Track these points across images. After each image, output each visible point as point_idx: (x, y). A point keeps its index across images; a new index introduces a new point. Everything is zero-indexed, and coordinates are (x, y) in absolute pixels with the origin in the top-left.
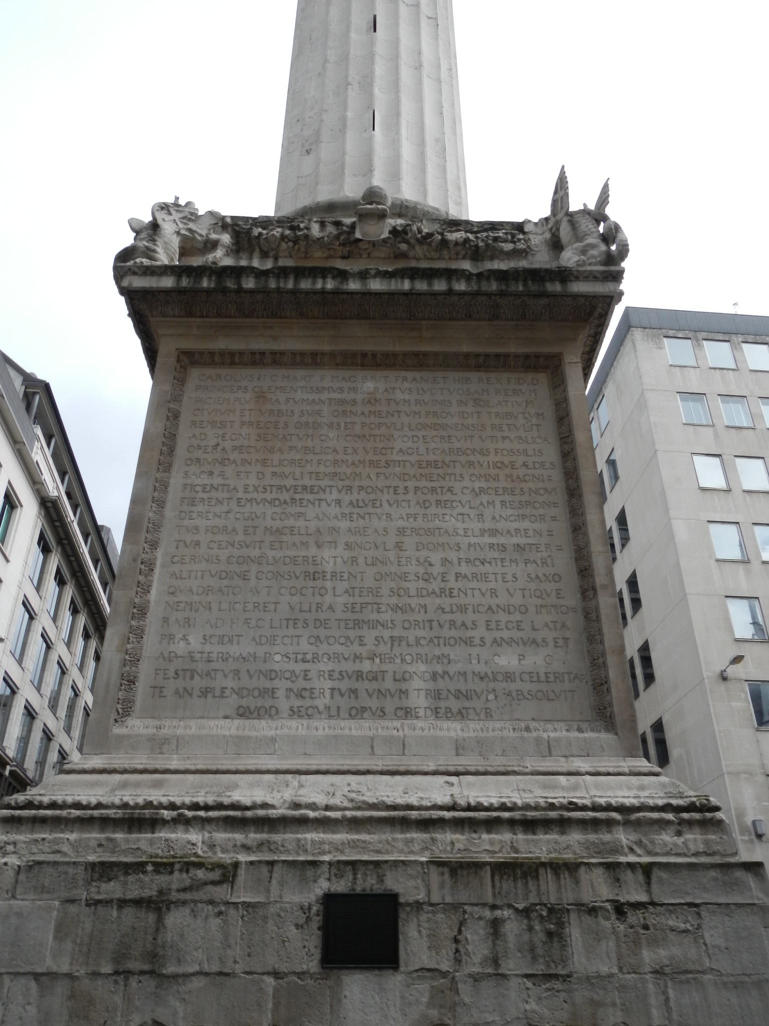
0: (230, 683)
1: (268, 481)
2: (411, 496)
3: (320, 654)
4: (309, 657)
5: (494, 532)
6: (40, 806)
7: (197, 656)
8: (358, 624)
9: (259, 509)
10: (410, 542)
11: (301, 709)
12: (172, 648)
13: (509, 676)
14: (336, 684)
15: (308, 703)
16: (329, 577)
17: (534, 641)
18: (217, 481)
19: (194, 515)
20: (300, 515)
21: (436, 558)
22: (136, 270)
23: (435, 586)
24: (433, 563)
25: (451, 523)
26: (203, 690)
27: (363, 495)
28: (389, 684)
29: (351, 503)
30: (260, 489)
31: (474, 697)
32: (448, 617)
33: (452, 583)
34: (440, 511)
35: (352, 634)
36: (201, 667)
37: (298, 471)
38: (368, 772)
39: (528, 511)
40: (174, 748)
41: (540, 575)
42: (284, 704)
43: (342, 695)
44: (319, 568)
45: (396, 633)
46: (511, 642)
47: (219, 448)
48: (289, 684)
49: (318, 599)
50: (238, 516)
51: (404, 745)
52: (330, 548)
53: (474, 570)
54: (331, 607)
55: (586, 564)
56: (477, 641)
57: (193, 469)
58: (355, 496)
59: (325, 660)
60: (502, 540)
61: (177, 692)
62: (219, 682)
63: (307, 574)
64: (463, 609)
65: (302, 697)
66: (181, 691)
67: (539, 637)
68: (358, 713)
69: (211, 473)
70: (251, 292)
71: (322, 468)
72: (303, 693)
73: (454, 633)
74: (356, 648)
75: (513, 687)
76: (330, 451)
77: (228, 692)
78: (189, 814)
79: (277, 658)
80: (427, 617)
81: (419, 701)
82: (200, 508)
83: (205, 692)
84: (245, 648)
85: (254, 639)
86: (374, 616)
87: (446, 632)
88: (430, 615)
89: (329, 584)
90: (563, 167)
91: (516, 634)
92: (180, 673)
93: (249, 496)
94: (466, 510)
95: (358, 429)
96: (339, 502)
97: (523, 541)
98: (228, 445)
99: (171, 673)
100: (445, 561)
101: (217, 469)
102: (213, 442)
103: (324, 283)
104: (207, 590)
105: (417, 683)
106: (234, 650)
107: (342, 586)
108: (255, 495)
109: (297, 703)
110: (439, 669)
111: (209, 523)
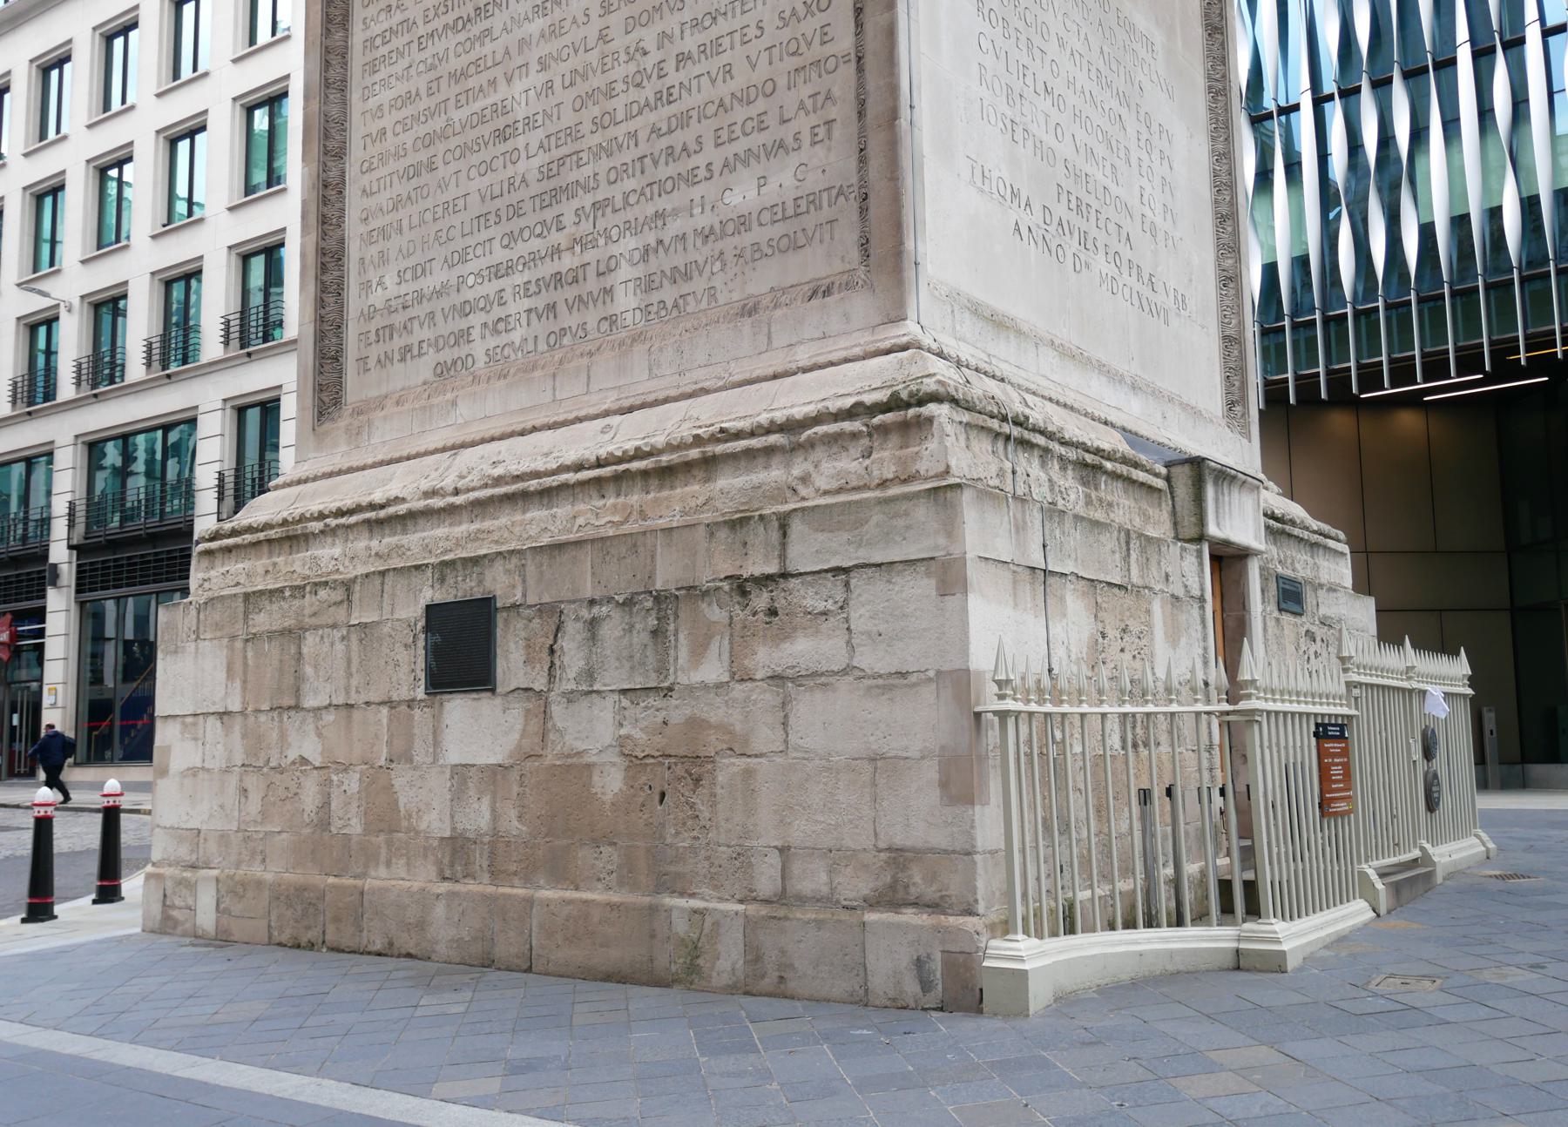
0: (427, 333)
13: (743, 223)
32: (664, 142)
33: (673, 78)
46: (746, 158)
56: (702, 173)
67: (787, 133)
74: (556, 238)
75: (747, 239)
78: (333, 522)
80: (639, 153)
87: (663, 172)
91: (756, 140)
99: (373, 337)
105: (625, 272)
106: (428, 283)
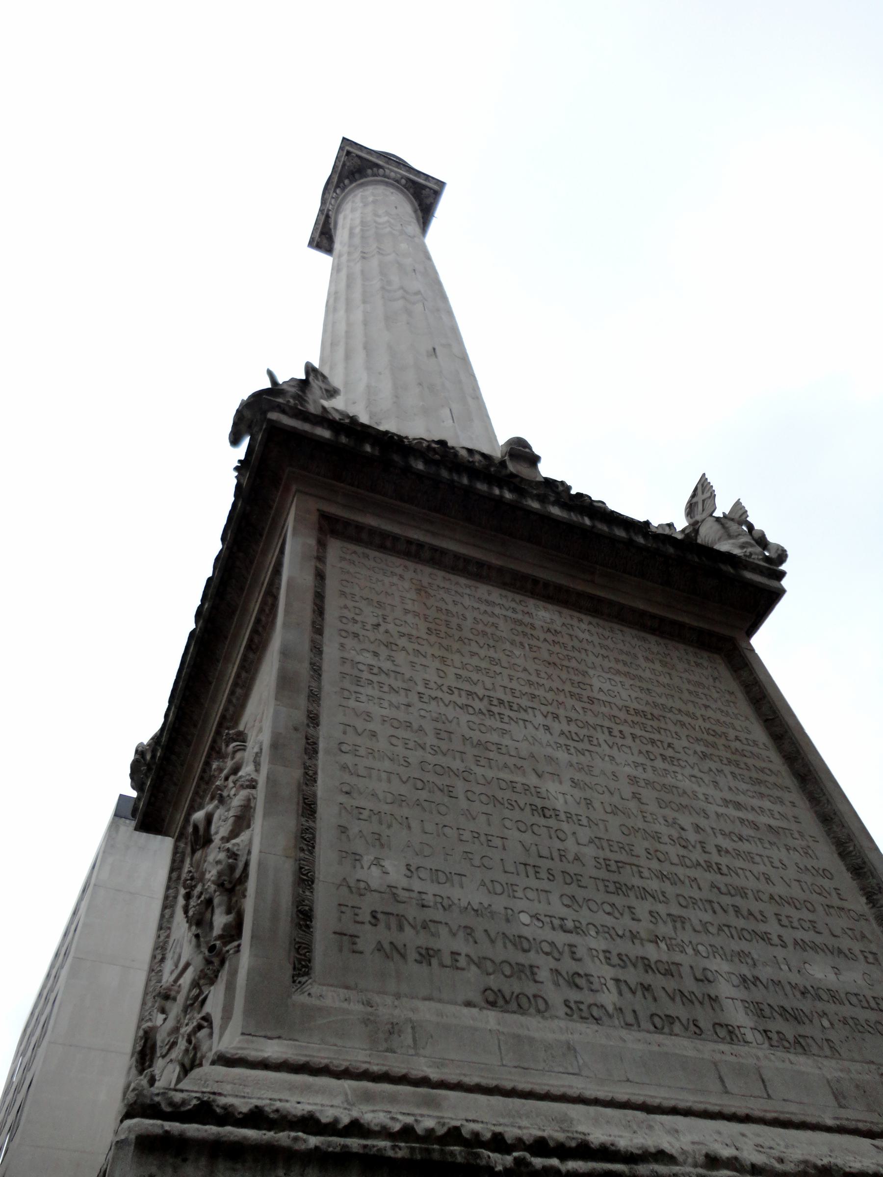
0: (461, 945)
1: (451, 681)
2: (629, 741)
3: (584, 923)
4: (569, 924)
5: (738, 806)
6: (227, 1117)
7: (403, 895)
8: (620, 889)
9: (451, 712)
10: (648, 795)
11: (582, 1006)
12: (360, 874)
14: (621, 974)
15: (589, 998)
16: (563, 816)
17: (840, 951)
18: (387, 665)
19: (363, 698)
20: (504, 732)
21: (685, 820)
22: (287, 409)
23: (697, 855)
24: (685, 828)
25: (686, 784)
26: (423, 952)
27: (573, 728)
28: (689, 985)
29: (562, 733)
30: (445, 688)
31: (807, 1022)
33: (715, 858)
34: (666, 766)
35: (619, 901)
36: (412, 912)
37: (488, 682)
38: (747, 1119)
39: (763, 789)
40: (410, 1041)
41: (809, 867)
42: (555, 996)
43: (634, 993)
44: (547, 804)
45: (676, 910)
47: (382, 629)
48: (553, 964)
49: (558, 844)
50: (423, 713)
51: (763, 1081)
52: (554, 781)
53: (735, 845)
54: (577, 858)
55: (859, 861)
57: (350, 642)
58: (565, 728)
59: (593, 933)
60: (751, 816)
61: (380, 948)
62: (445, 943)
63: (534, 808)
64: (742, 893)
65: (577, 986)
66: (387, 946)
68: (664, 1024)
69: (376, 654)
70: (419, 475)
71: (514, 685)
72: (578, 980)
73: (741, 923)
76: (520, 669)
77: (462, 962)
79: (525, 918)
81: (738, 1016)
82: (369, 691)
83: (427, 956)
84: (469, 894)
85: (483, 884)
86: (636, 881)
88: (706, 894)
89: (565, 826)
90: (704, 474)
92: (379, 916)
93: (434, 694)
94: (696, 772)
95: (545, 655)
96: (547, 728)
97: (774, 823)
98: (391, 627)
100: (698, 828)
101: (384, 652)
102: (375, 621)
103: (501, 492)
104: (400, 800)
107: (584, 834)
108: (439, 694)
109: (574, 996)
110: (745, 971)
111: (385, 712)
